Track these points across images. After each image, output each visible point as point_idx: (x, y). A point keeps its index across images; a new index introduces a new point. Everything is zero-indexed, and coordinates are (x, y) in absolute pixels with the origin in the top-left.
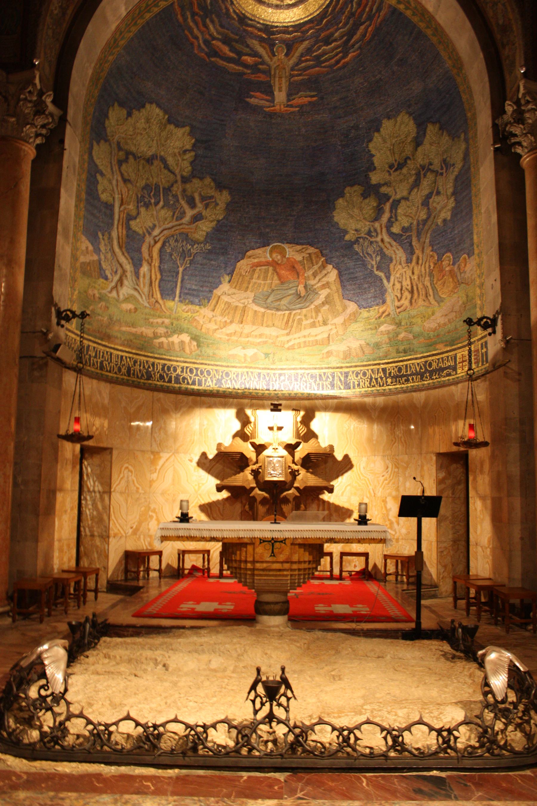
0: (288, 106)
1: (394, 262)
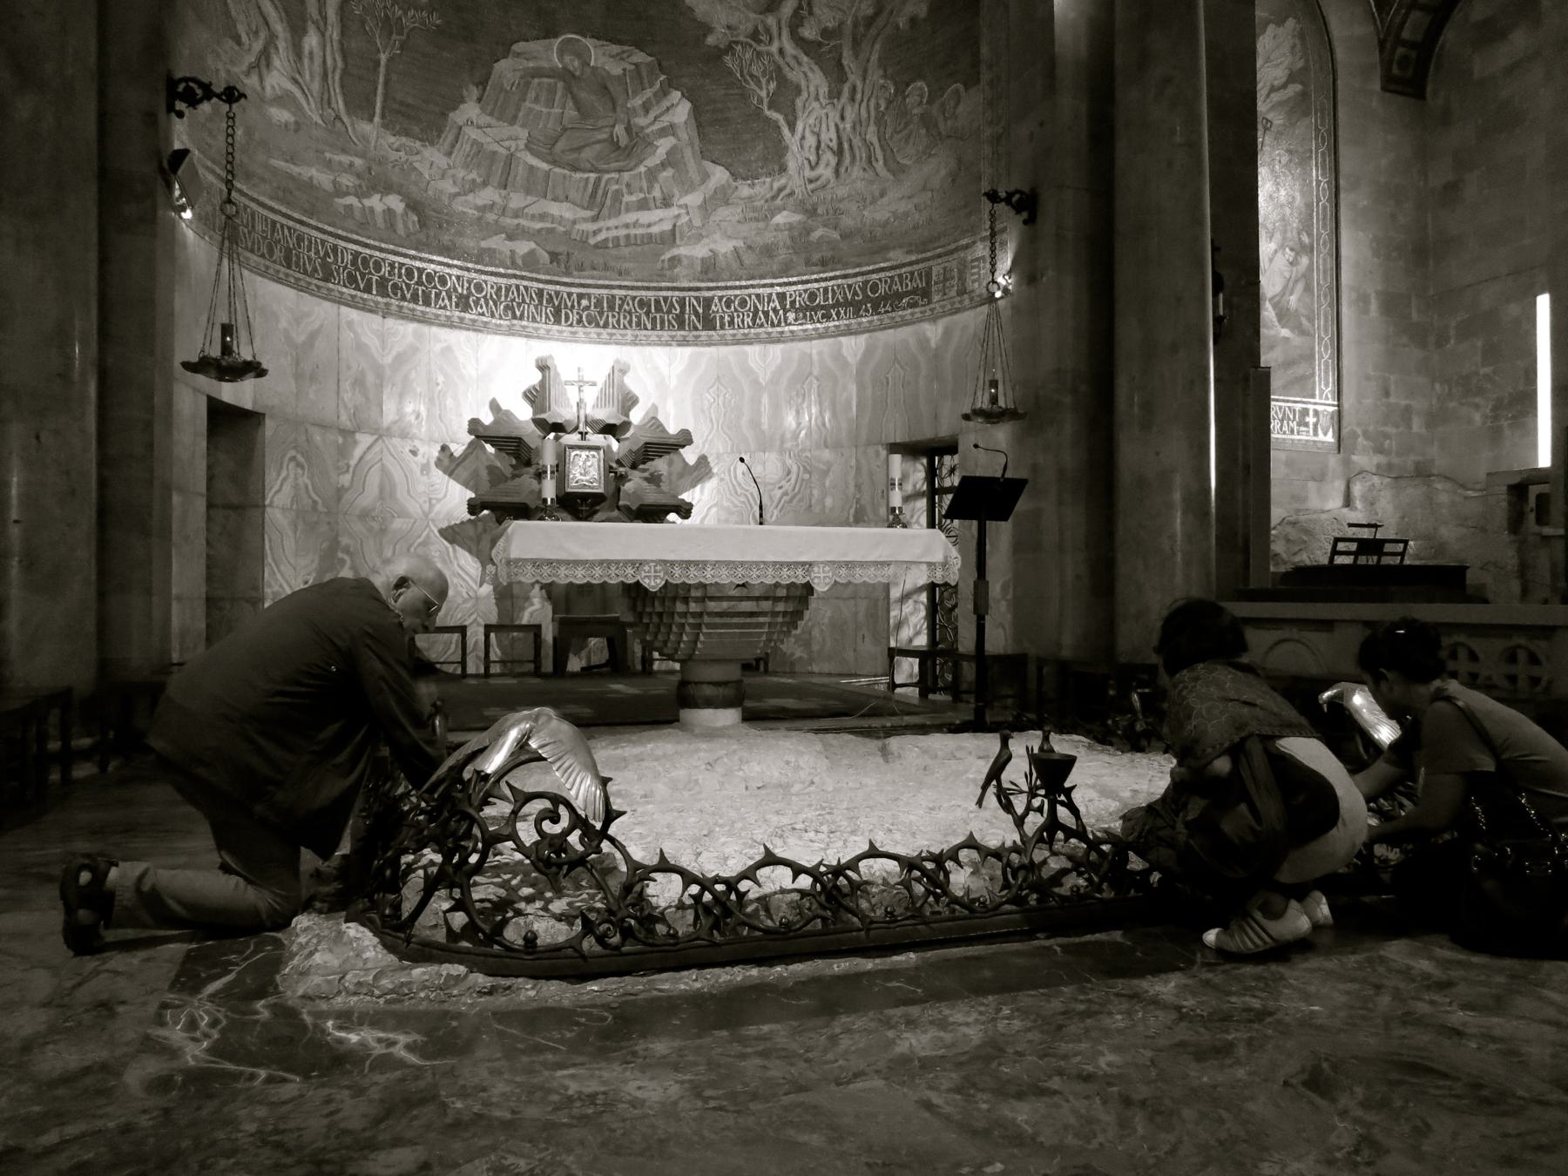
1: (805, 94)
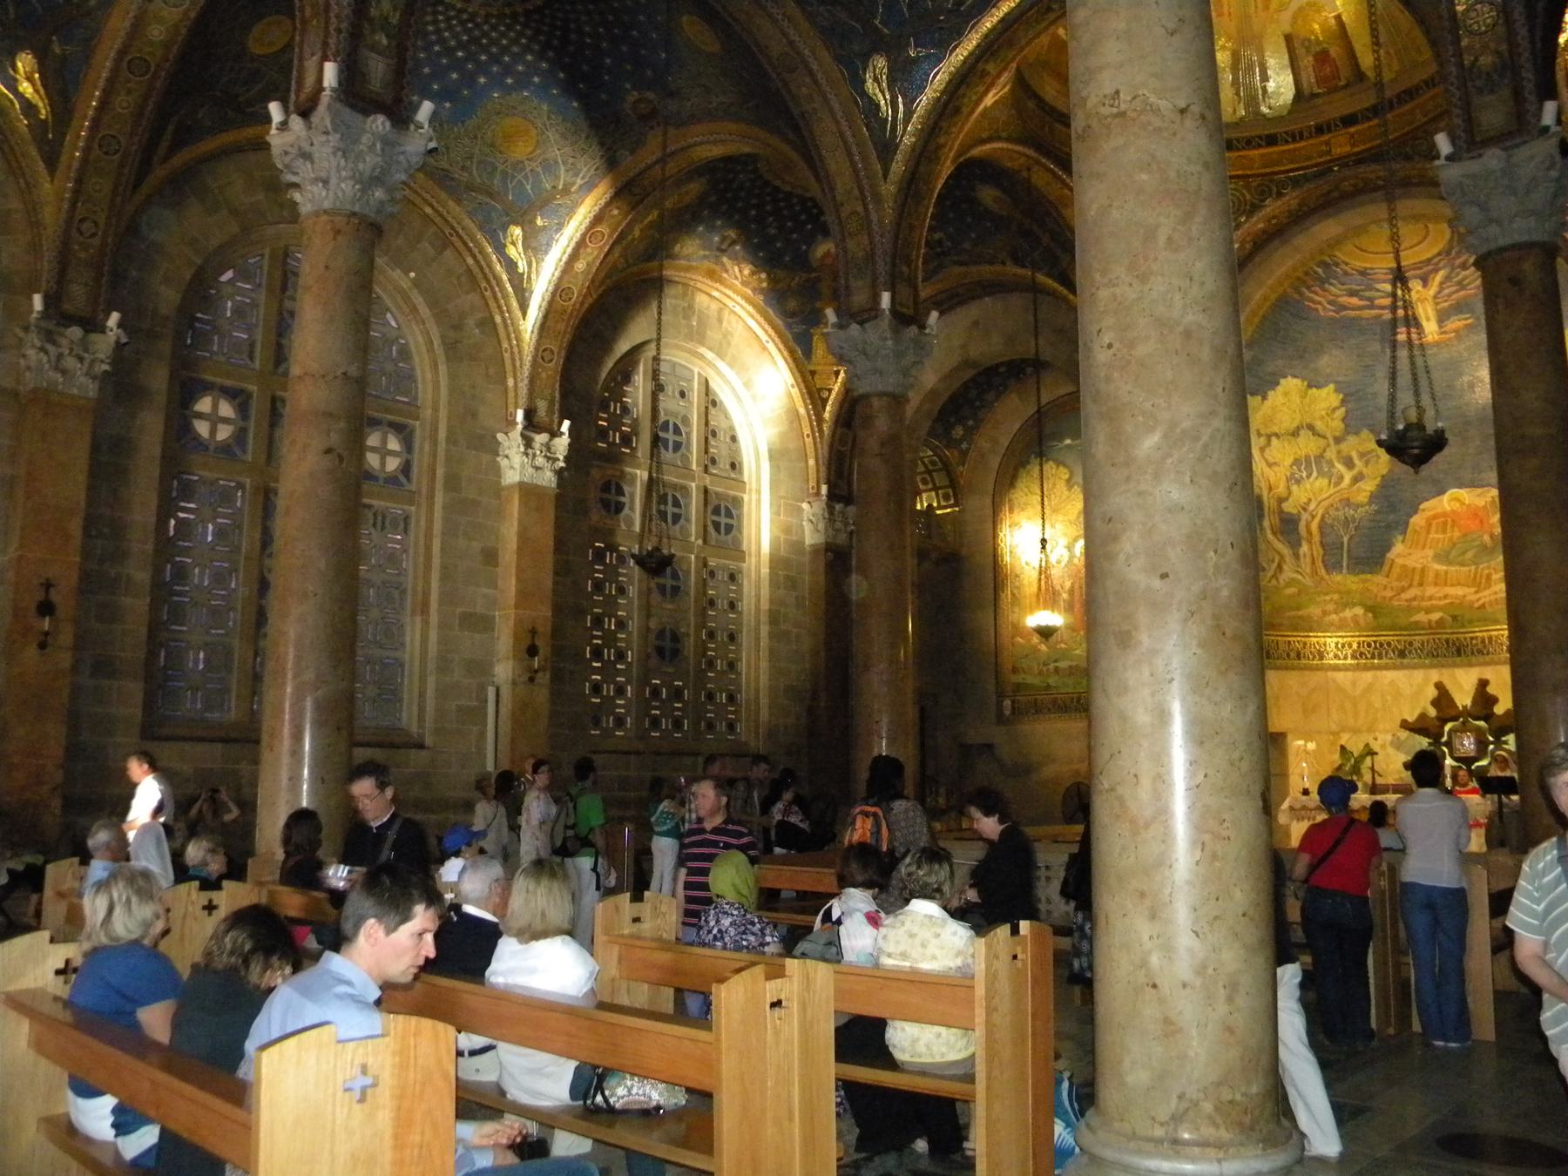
0: (1442, 333)
